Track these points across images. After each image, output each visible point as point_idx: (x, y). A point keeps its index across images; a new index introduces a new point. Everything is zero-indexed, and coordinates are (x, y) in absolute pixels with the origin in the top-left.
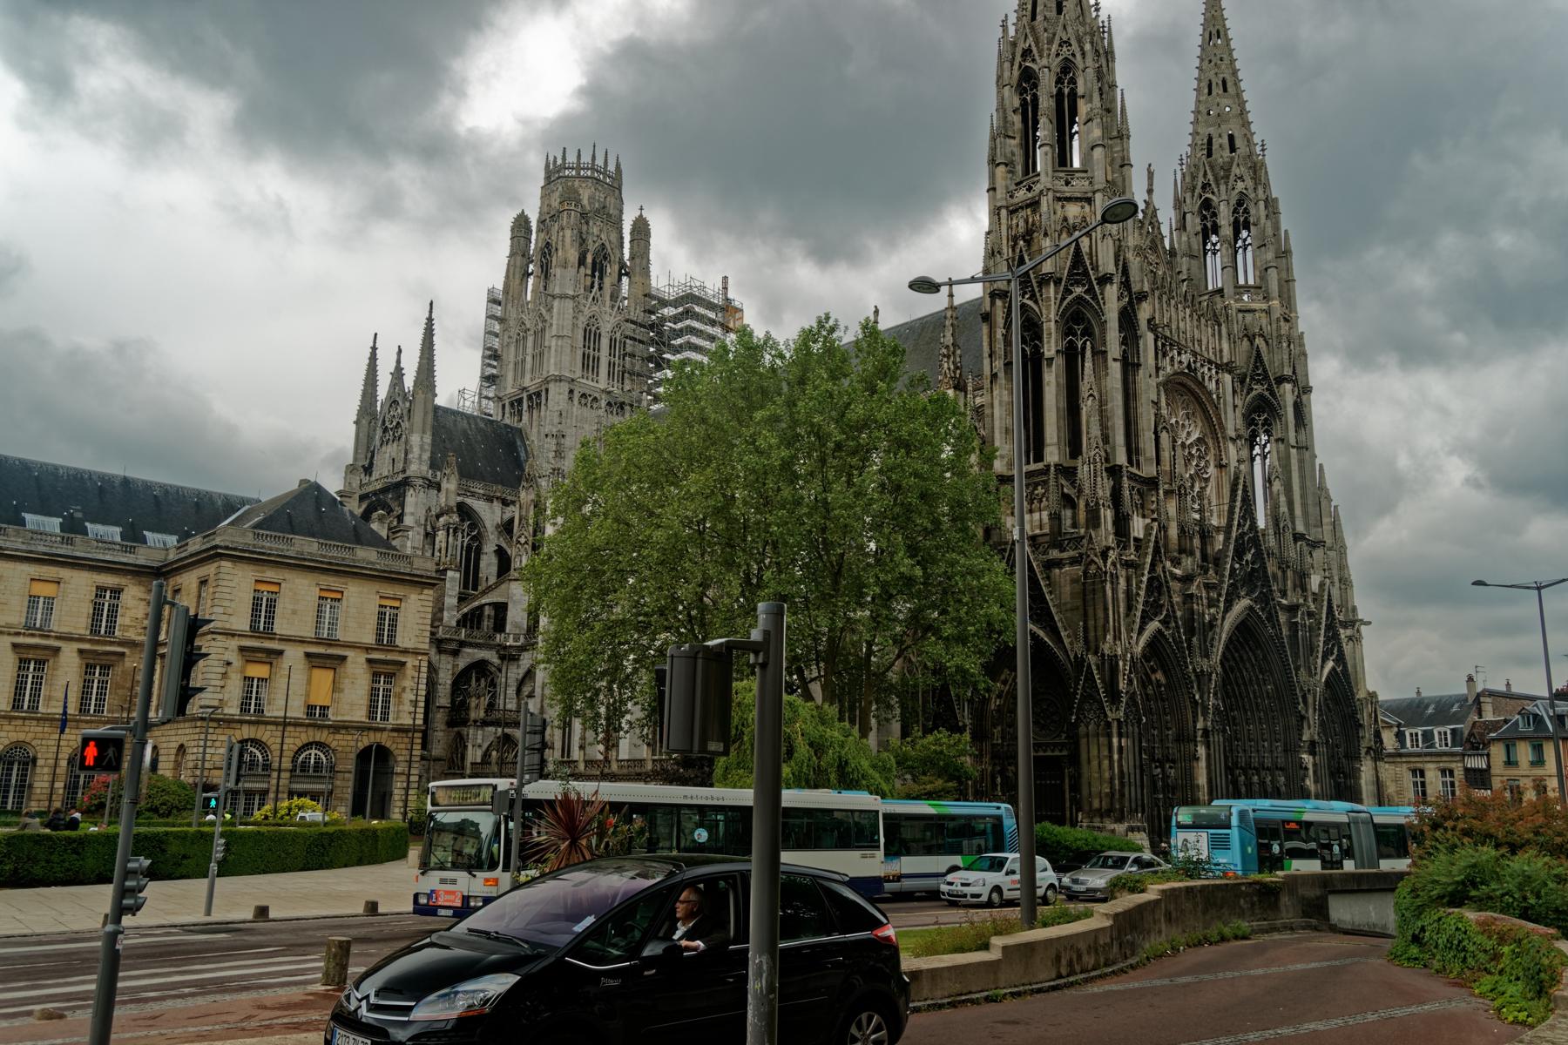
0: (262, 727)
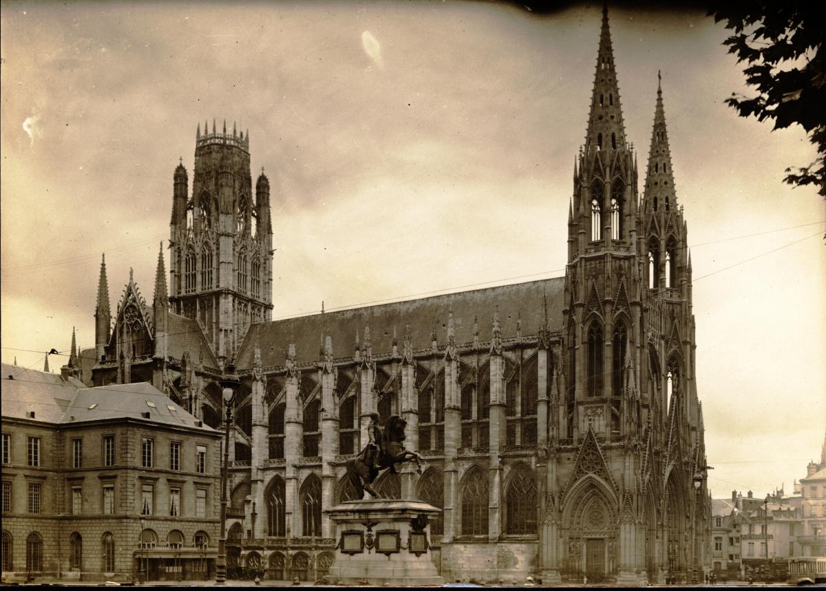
0: (152, 522)
